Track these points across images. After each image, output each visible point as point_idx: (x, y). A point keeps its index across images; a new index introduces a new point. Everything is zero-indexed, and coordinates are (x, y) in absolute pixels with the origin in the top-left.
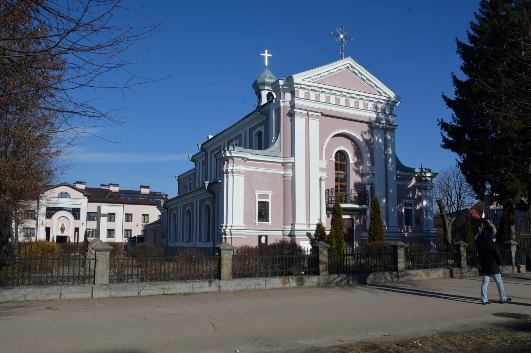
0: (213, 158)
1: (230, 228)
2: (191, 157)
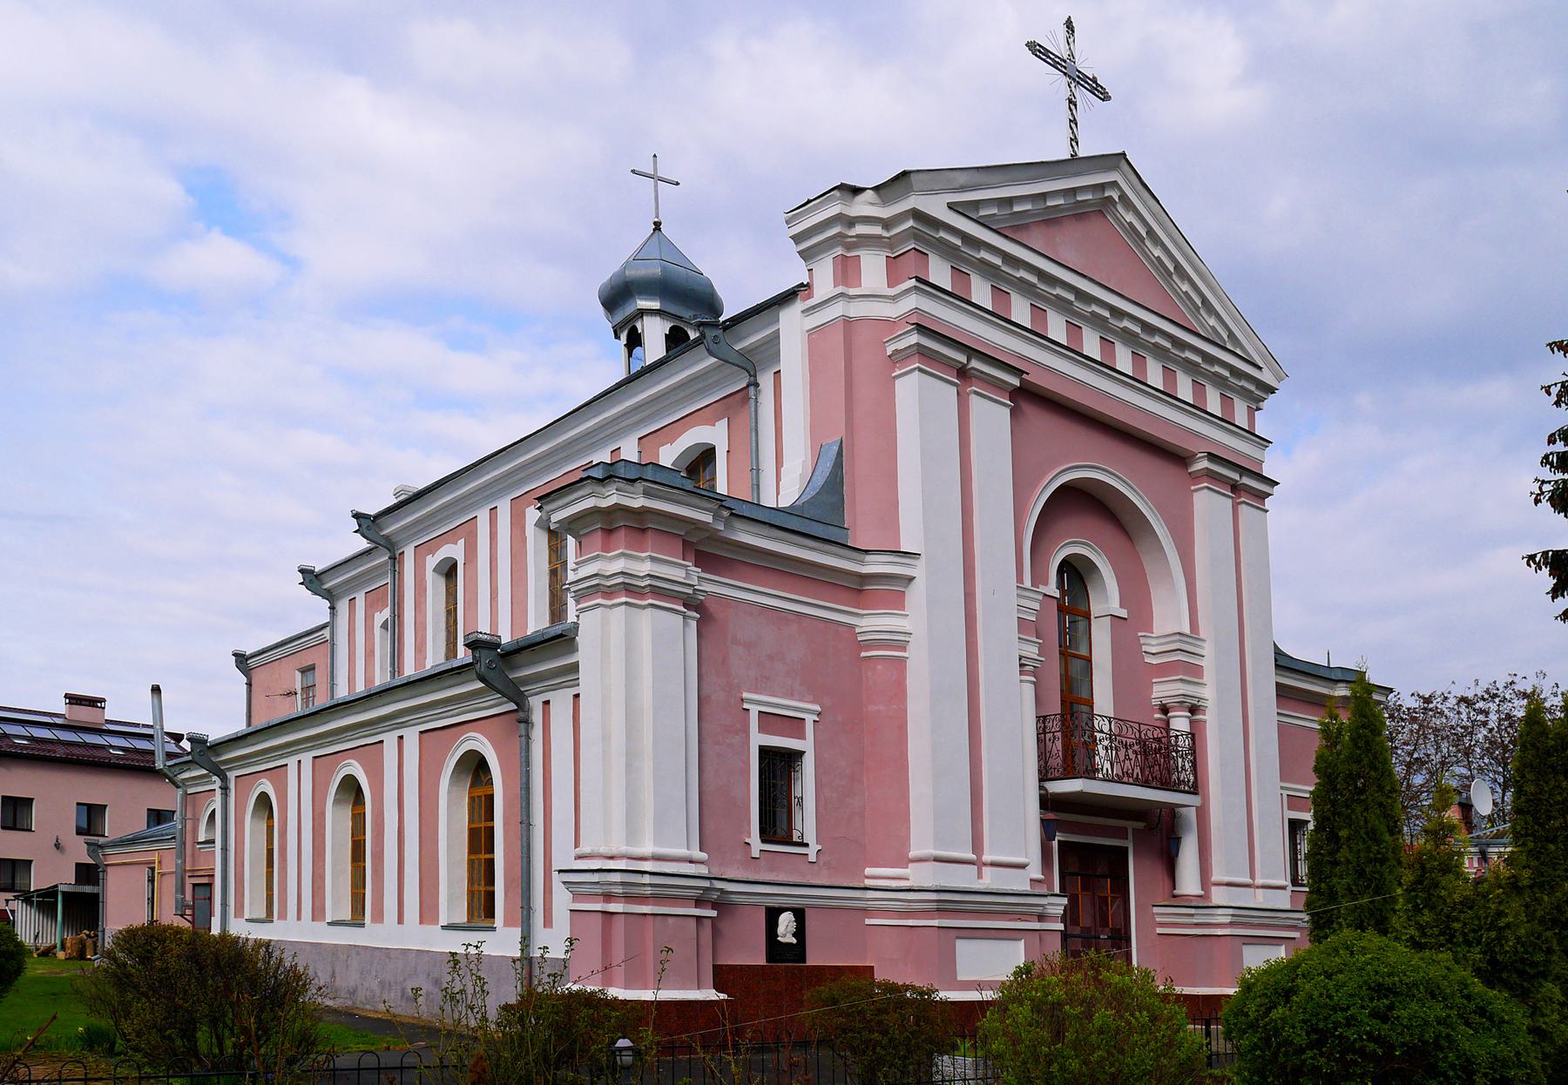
0: (430, 575)
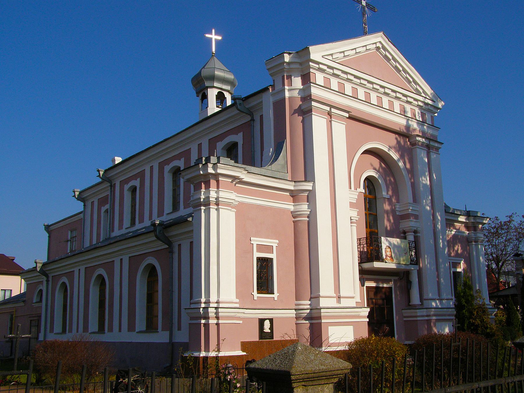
1: (215, 305)
2: (77, 193)
